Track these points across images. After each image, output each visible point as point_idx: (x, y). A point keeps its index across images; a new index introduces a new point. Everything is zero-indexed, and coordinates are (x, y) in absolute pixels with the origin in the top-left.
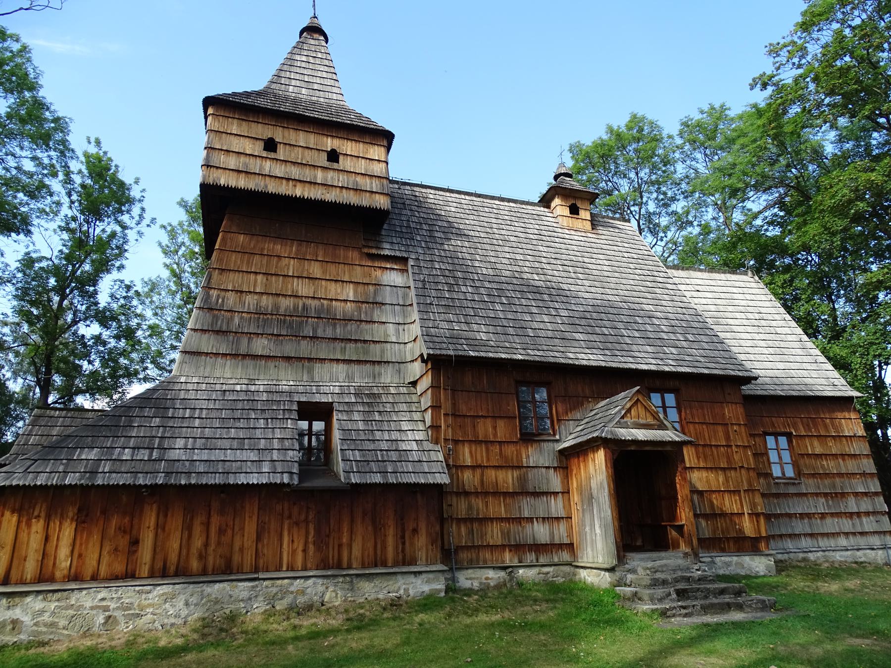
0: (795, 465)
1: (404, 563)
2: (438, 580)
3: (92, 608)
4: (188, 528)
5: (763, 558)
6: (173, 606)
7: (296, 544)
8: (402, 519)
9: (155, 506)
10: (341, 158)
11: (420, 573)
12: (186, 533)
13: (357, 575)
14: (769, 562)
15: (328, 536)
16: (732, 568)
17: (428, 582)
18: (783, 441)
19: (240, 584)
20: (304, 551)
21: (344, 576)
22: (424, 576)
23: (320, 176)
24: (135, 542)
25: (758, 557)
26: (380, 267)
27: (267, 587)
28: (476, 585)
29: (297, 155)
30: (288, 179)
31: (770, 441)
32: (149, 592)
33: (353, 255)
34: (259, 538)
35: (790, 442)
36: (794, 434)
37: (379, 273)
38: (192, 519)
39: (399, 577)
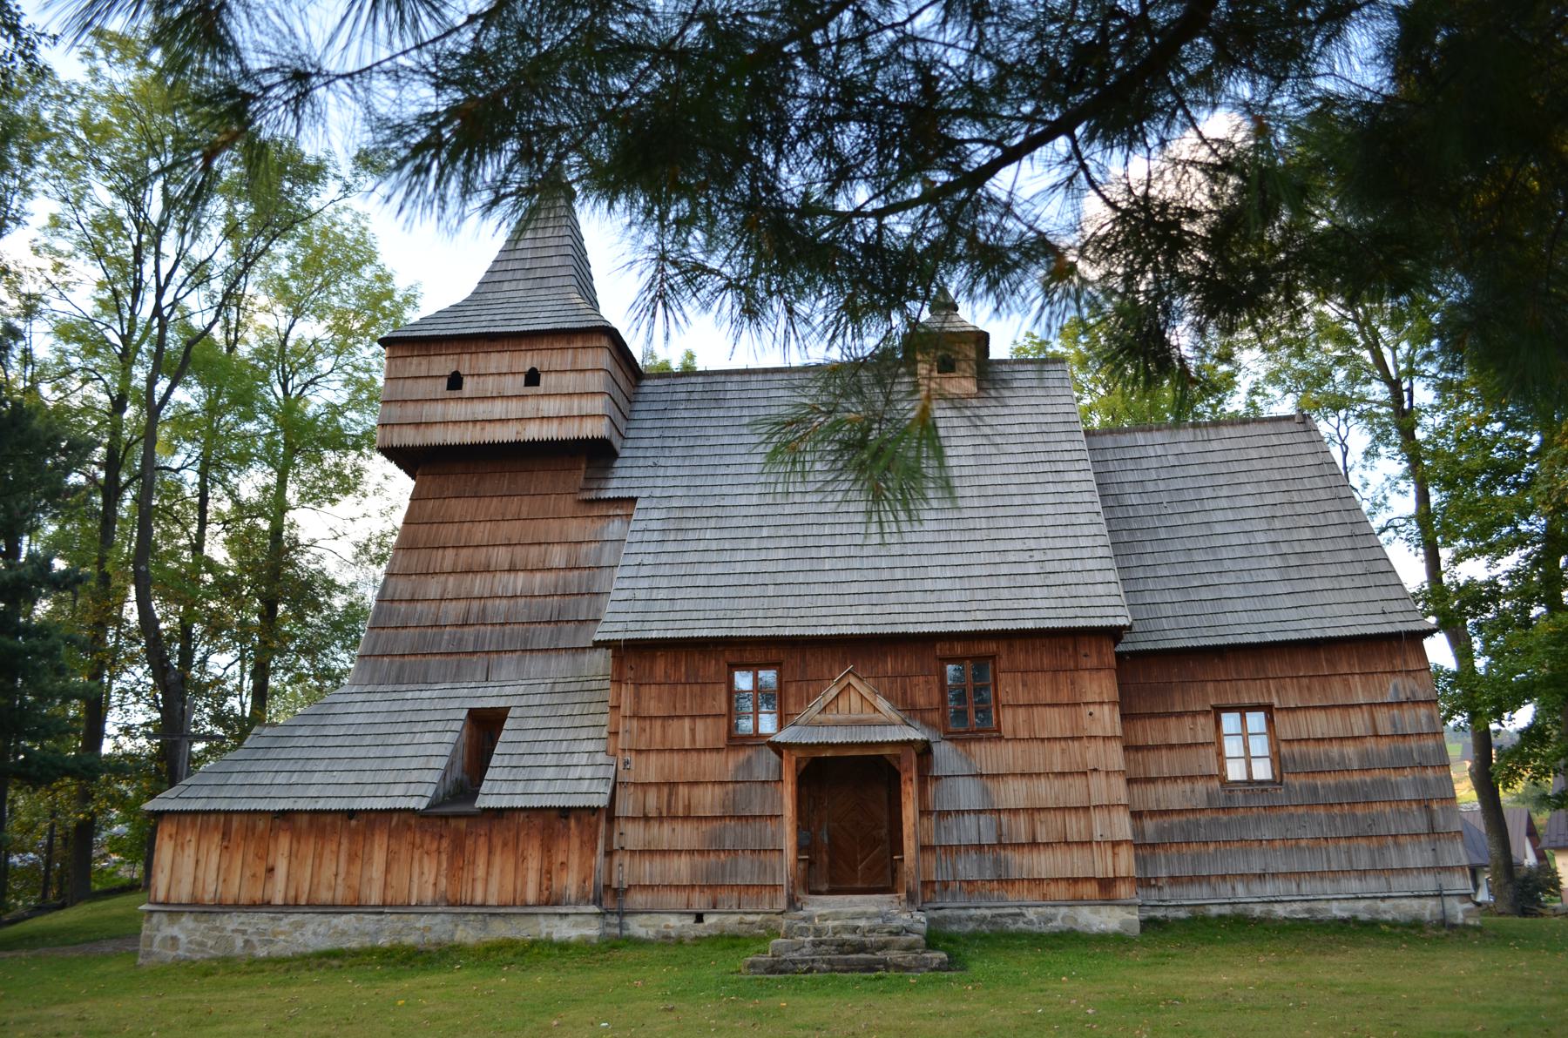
0: (1277, 758)
1: (547, 904)
2: (589, 925)
3: (233, 931)
4: (318, 856)
5: (1116, 908)
6: (302, 935)
7: (425, 877)
8: (549, 851)
9: (312, 841)
10: (543, 378)
11: (567, 915)
12: (317, 861)
13: (492, 914)
14: (1130, 917)
15: (462, 869)
16: (1054, 924)
17: (576, 925)
18: (1256, 721)
19: (366, 916)
20: (435, 884)
21: (476, 914)
22: (571, 918)
23: (514, 408)
24: (271, 870)
25: (1108, 908)
26: (600, 517)
27: (392, 921)
28: (652, 933)
29: (490, 385)
30: (475, 422)
31: (1230, 722)
32: (281, 920)
33: (567, 504)
34: (387, 870)
35: (1270, 722)
36: (1277, 705)
37: (599, 524)
38: (323, 847)
39: (541, 919)
